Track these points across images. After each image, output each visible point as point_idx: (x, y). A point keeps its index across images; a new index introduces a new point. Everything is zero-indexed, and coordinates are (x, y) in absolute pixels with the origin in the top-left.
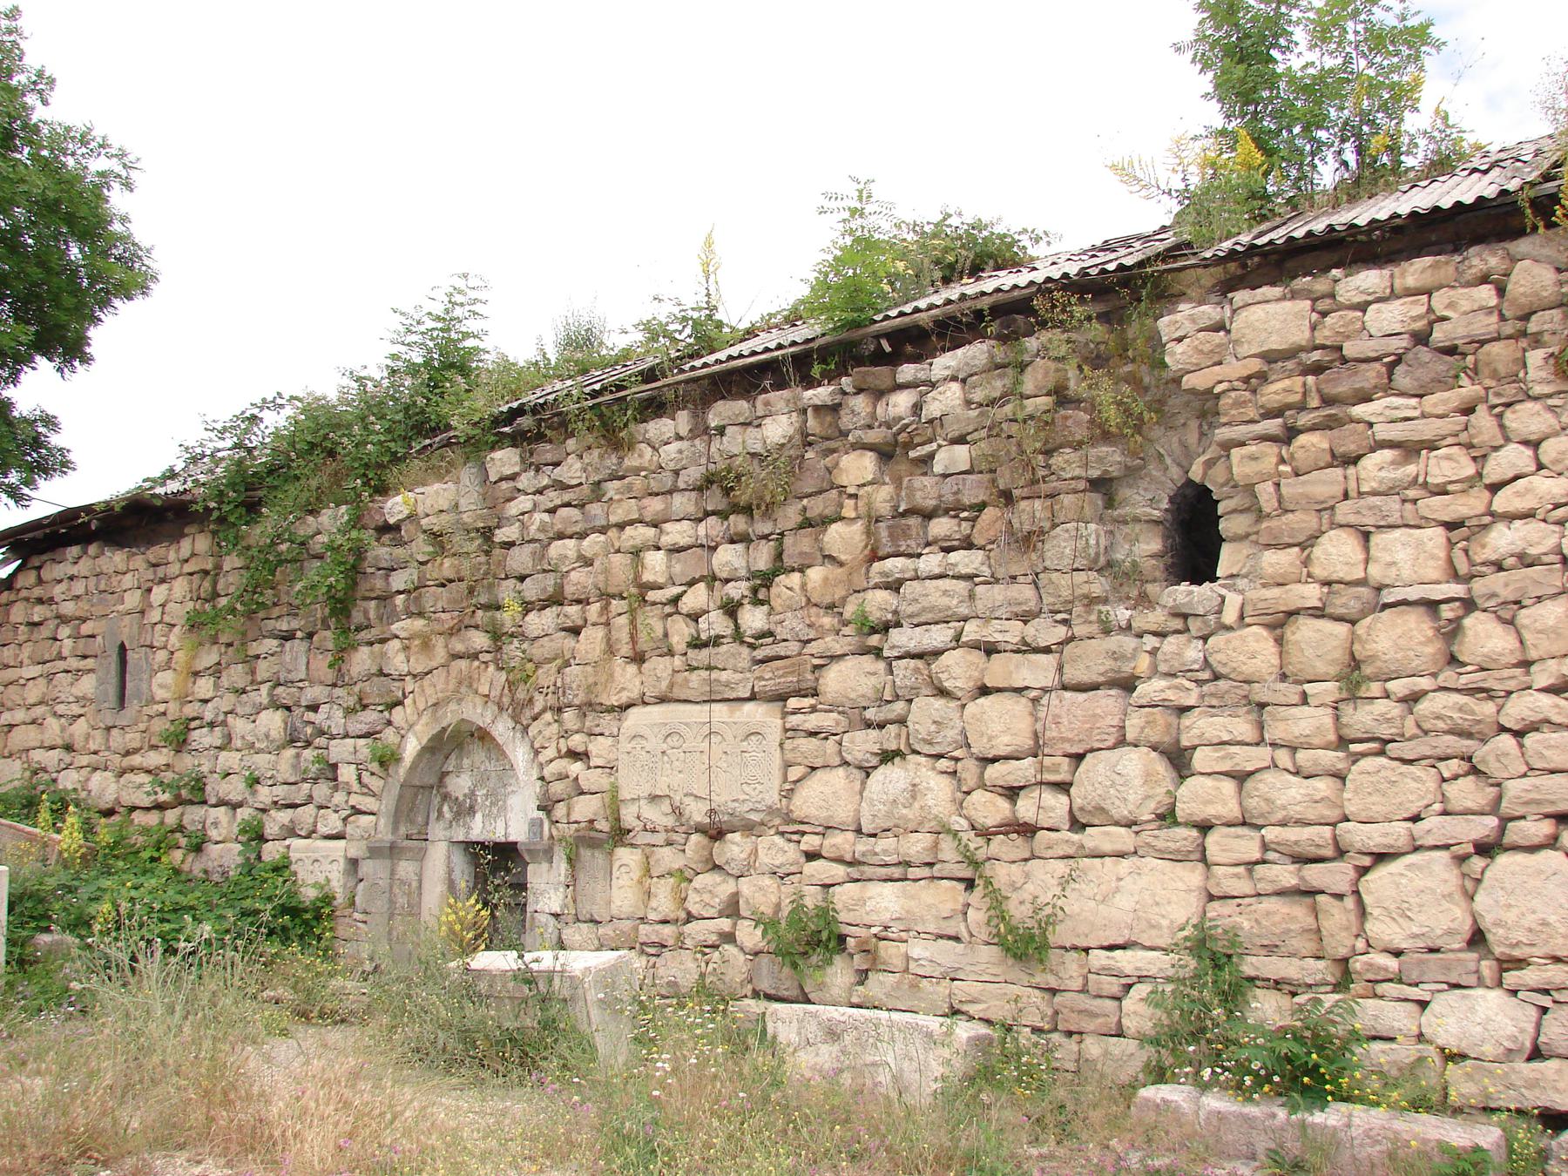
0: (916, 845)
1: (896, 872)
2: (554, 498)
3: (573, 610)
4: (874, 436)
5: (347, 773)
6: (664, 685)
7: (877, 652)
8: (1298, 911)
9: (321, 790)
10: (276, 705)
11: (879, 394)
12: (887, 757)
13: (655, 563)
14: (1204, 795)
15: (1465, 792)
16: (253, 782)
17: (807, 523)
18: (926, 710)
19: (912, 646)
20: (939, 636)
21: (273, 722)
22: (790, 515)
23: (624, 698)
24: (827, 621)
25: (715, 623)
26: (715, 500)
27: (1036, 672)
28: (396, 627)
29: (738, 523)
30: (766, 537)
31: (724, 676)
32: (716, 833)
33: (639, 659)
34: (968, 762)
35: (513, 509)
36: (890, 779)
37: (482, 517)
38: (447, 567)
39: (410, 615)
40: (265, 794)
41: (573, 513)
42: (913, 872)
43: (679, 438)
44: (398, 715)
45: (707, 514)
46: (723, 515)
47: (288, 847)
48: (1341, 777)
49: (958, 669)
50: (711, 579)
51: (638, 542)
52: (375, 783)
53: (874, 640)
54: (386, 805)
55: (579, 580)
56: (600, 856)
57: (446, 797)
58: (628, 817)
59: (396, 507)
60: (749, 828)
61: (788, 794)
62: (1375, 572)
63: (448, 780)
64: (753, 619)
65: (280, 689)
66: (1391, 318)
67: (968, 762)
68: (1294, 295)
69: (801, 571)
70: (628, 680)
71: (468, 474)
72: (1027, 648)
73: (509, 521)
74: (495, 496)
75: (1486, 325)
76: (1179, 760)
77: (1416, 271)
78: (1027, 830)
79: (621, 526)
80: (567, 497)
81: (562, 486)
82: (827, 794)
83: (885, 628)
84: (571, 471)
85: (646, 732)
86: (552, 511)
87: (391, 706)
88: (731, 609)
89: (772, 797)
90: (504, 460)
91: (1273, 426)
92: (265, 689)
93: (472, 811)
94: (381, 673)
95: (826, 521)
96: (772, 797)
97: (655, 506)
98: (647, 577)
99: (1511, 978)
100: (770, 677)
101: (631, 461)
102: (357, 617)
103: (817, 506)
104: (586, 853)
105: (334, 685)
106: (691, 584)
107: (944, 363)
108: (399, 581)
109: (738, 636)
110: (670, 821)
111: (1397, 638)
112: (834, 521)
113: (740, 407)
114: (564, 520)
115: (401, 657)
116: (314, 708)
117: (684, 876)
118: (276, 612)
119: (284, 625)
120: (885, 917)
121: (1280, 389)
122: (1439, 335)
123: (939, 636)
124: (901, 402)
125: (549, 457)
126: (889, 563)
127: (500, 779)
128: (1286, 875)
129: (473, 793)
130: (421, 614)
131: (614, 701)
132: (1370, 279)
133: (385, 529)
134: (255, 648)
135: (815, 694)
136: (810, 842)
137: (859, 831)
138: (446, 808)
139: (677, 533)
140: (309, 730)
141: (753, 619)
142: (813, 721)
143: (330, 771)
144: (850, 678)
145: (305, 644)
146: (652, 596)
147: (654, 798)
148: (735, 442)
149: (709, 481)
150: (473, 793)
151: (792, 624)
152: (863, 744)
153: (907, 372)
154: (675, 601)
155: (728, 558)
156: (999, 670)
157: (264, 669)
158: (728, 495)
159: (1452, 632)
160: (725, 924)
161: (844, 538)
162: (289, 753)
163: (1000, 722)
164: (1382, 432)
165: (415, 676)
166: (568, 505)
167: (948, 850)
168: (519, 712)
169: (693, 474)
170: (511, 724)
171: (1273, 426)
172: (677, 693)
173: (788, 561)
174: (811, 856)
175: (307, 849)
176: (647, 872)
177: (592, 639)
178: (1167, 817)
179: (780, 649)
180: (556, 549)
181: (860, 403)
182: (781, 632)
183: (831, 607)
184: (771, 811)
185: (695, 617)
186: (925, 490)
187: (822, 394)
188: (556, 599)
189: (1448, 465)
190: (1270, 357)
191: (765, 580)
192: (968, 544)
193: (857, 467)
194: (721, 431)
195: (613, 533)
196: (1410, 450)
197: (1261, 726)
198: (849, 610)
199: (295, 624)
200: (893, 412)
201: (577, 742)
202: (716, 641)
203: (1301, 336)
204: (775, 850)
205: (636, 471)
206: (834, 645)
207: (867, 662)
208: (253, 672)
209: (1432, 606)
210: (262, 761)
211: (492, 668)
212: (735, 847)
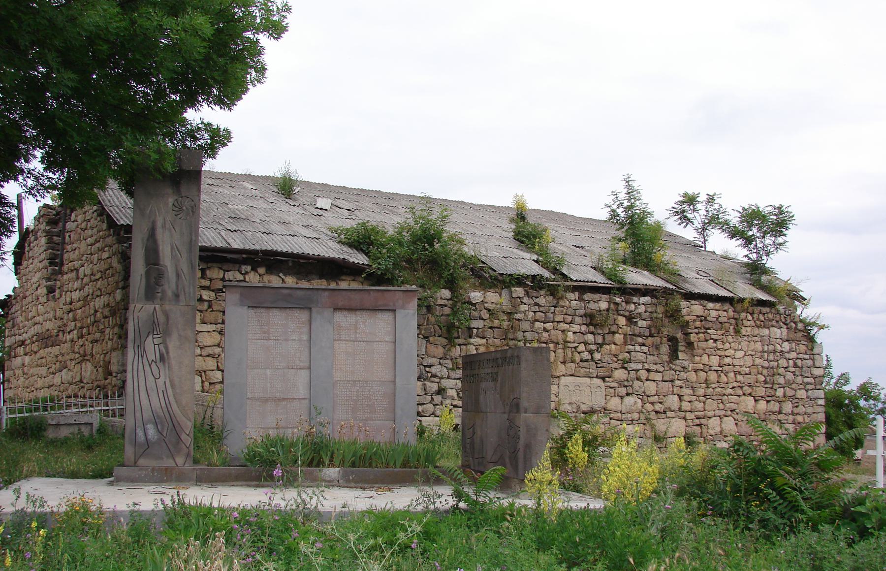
0: (636, 416)
4: (627, 314)
7: (626, 368)
8: (698, 428)
9: (438, 399)
11: (627, 303)
12: (628, 394)
14: (686, 406)
15: (721, 406)
18: (637, 384)
20: (640, 366)
27: (658, 377)
28: (472, 340)
29: (592, 328)
33: (564, 363)
34: (644, 396)
35: (523, 308)
38: (496, 323)
39: (478, 336)
46: (587, 325)
48: (704, 403)
49: (643, 374)
50: (586, 343)
62: (711, 364)
64: (597, 356)
66: (714, 314)
67: (644, 396)
68: (701, 305)
71: (505, 292)
72: (657, 371)
74: (515, 302)
75: (725, 320)
76: (680, 397)
77: (718, 305)
78: (657, 412)
79: (558, 322)
81: (536, 304)
88: (591, 352)
89: (603, 404)
90: (519, 291)
91: (696, 331)
95: (614, 333)
98: (568, 339)
99: (726, 439)
101: (561, 303)
107: (643, 300)
109: (592, 359)
111: (713, 376)
116: (430, 366)
121: (698, 324)
122: (720, 319)
123: (640, 366)
125: (535, 295)
128: (697, 421)
130: (483, 338)
131: (558, 374)
132: (710, 305)
141: (597, 356)
144: (620, 374)
146: (569, 345)
147: (570, 403)
148: (592, 306)
149: (585, 315)
151: (607, 358)
152: (623, 391)
154: (575, 348)
155: (590, 337)
156: (652, 376)
158: (592, 320)
159: (719, 376)
161: (619, 338)
163: (651, 388)
164: (713, 337)
167: (642, 416)
169: (582, 312)
171: (696, 331)
175: (432, 421)
178: (680, 410)
179: (604, 365)
180: (537, 324)
181: (624, 304)
182: (604, 360)
186: (637, 330)
189: (719, 345)
190: (698, 316)
191: (601, 345)
192: (644, 345)
193: (622, 321)
194: (589, 302)
196: (715, 341)
197: (694, 391)
202: (587, 361)
203: (702, 314)
205: (563, 307)
206: (615, 365)
209: (717, 371)
212: (595, 417)
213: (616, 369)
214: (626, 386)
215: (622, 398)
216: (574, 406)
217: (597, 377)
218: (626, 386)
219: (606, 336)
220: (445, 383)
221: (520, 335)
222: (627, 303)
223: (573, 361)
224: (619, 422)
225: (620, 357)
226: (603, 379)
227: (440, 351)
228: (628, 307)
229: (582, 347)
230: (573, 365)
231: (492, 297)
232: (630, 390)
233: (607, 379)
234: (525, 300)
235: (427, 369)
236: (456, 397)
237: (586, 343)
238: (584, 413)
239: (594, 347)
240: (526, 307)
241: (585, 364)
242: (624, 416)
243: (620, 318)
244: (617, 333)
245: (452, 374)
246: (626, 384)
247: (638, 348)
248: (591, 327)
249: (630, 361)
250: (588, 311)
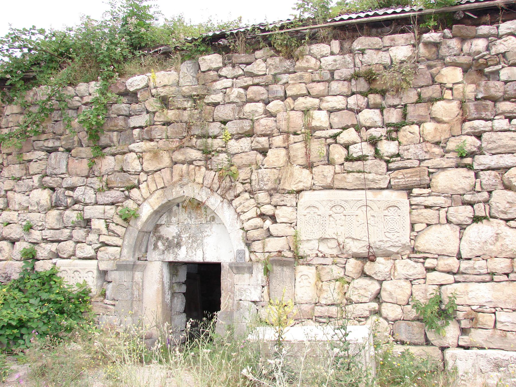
1: (488, 278)
2: (249, 81)
3: (264, 140)
4: (464, 59)
5: (96, 224)
6: (329, 180)
7: (470, 167)
9: (79, 233)
10: (43, 186)
11: (463, 39)
12: (476, 219)
13: (320, 118)
16: (29, 228)
17: (420, 100)
19: (493, 164)
21: (43, 196)
22: (411, 96)
23: (300, 186)
24: (437, 150)
25: (368, 150)
26: (362, 85)
28: (132, 146)
30: (395, 106)
31: (370, 176)
32: (370, 258)
33: (310, 166)
35: (219, 85)
36: (478, 233)
37: (196, 90)
38: (171, 114)
39: (143, 140)
40: (36, 235)
41: (262, 89)
42: (496, 278)
43: (332, 54)
44: (135, 193)
45: (353, 94)
46: (364, 95)
47: (55, 264)
51: (309, 105)
52: (120, 230)
53: (468, 160)
54: (130, 240)
55: (265, 124)
56: (287, 271)
57: (159, 238)
58: (304, 249)
59: (135, 82)
60: (387, 255)
61: (414, 239)
63: (161, 229)
64: (388, 148)
65: (47, 179)
69: (419, 124)
70: (301, 177)
71: (186, 67)
73: (216, 92)
79: (295, 98)
80: (256, 80)
81: (252, 75)
82: (439, 238)
83: (472, 154)
84: (259, 67)
85: (317, 205)
86: (246, 88)
87: (130, 188)
88: (374, 142)
89: (405, 239)
90: (212, 60)
92: (36, 178)
93: (178, 245)
94: (122, 170)
95: (432, 101)
96: (405, 239)
97: (320, 87)
98: (314, 124)
100: (400, 178)
102: (104, 140)
103: (427, 93)
104: (277, 269)
105: (87, 177)
106: (344, 129)
108: (134, 122)
109: (377, 155)
110: (335, 252)
112: (439, 100)
113: (375, 40)
114: (254, 93)
115: (137, 162)
116: (73, 189)
117: (345, 281)
118: (44, 137)
119: (50, 144)
120: (482, 301)
124: (480, 44)
125: (243, 60)
126: (476, 123)
127: (198, 228)
129: (179, 236)
130: (151, 140)
131: (294, 188)
133: (126, 93)
134: (28, 156)
135: (429, 187)
136: (429, 263)
137: (459, 257)
138: (160, 244)
139: (338, 102)
140: (69, 200)
141: (388, 148)
142: (430, 201)
143: (87, 223)
145: (65, 155)
146: (318, 133)
147: (322, 240)
148: (373, 58)
149: (356, 76)
150: (179, 236)
151: (413, 151)
152: (464, 213)
153: (484, 29)
154: (335, 137)
155: (369, 116)
157: (34, 167)
158: (370, 82)
160: (375, 305)
162: (55, 213)
165: (146, 173)
166: (257, 85)
168: (227, 194)
169: (347, 72)
170: (220, 199)
172: (337, 184)
173: (409, 118)
174: (429, 270)
175: (70, 265)
176: (319, 278)
177: (277, 156)
179: (408, 163)
180: (249, 107)
181: (454, 43)
182: (406, 155)
183: (437, 143)
184: (404, 246)
185: (347, 147)
186: (496, 88)
187: (432, 36)
188: (250, 134)
191: (397, 127)
193: (452, 75)
194: (362, 52)
195: (289, 100)
198: (452, 145)
199: (57, 144)
200: (474, 48)
201: (268, 209)
202: (362, 158)
204: (407, 267)
205: (306, 69)
206: (437, 161)
207: (463, 171)
208: (27, 169)
210: (35, 217)
211: (203, 169)
212: (381, 266)
213: (443, 169)
214: (471, 204)
215: (462, 227)
216: (333, 244)
217: (389, 187)
218: (471, 204)
219: (410, 109)
220: (89, 212)
221: (214, 128)
222: (463, 39)
223: (330, 162)
224: (451, 278)
225: (452, 145)
226: (408, 190)
227: (83, 166)
228: (466, 47)
229: (350, 135)
230: (328, 170)
231: (163, 79)
232: (480, 210)
233: (416, 191)
234: (224, 72)
235: (67, 193)
236: (104, 231)
237: (358, 128)
238: (357, 257)
239: (376, 133)
240: (227, 83)
241: (357, 165)
242: (464, 265)
243: (445, 71)
244: (442, 99)
245: (101, 198)
246: (468, 197)
247: (501, 123)
248: (371, 96)
249: (480, 151)
250: (363, 69)
